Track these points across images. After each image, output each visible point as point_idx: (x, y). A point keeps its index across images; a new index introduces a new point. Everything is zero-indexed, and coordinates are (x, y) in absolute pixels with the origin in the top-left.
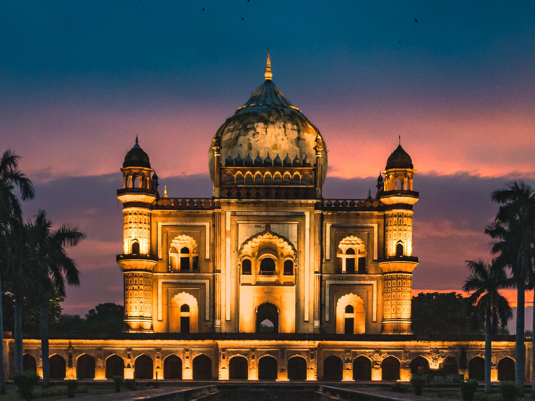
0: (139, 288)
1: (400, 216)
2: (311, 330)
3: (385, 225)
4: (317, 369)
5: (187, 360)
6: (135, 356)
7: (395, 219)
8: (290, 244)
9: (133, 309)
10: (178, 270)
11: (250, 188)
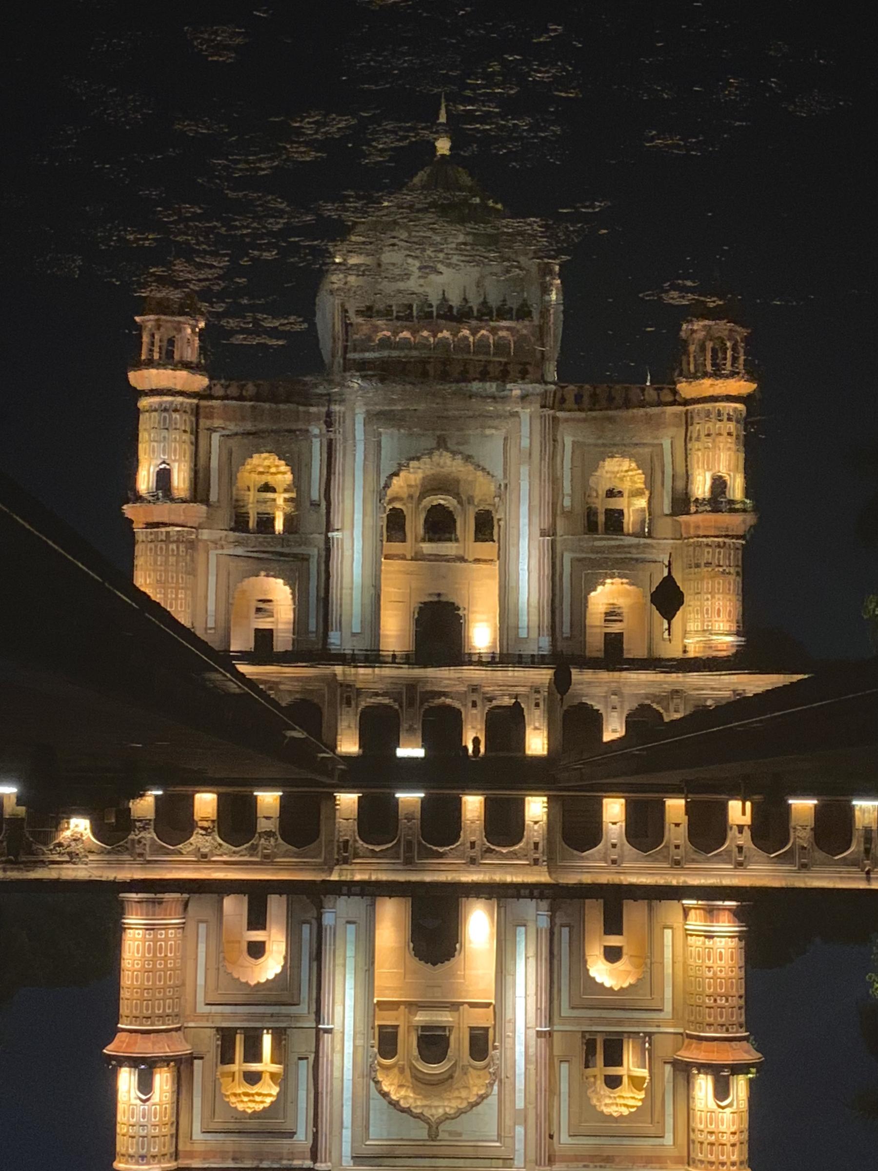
0: (715, 1000)
4: (335, 818)
5: (614, 841)
6: (728, 852)
7: (154, 1151)
8: (385, 1095)
9: (726, 954)
10: (629, 1038)
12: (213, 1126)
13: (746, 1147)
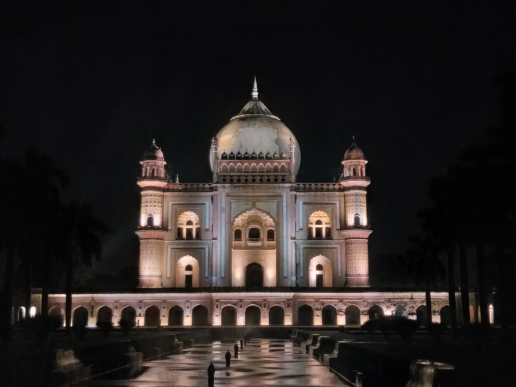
1: (357, 195)
2: (289, 284)
3: (345, 202)
7: (353, 197)
11: (240, 176)
12: (333, 206)
13: (142, 202)
